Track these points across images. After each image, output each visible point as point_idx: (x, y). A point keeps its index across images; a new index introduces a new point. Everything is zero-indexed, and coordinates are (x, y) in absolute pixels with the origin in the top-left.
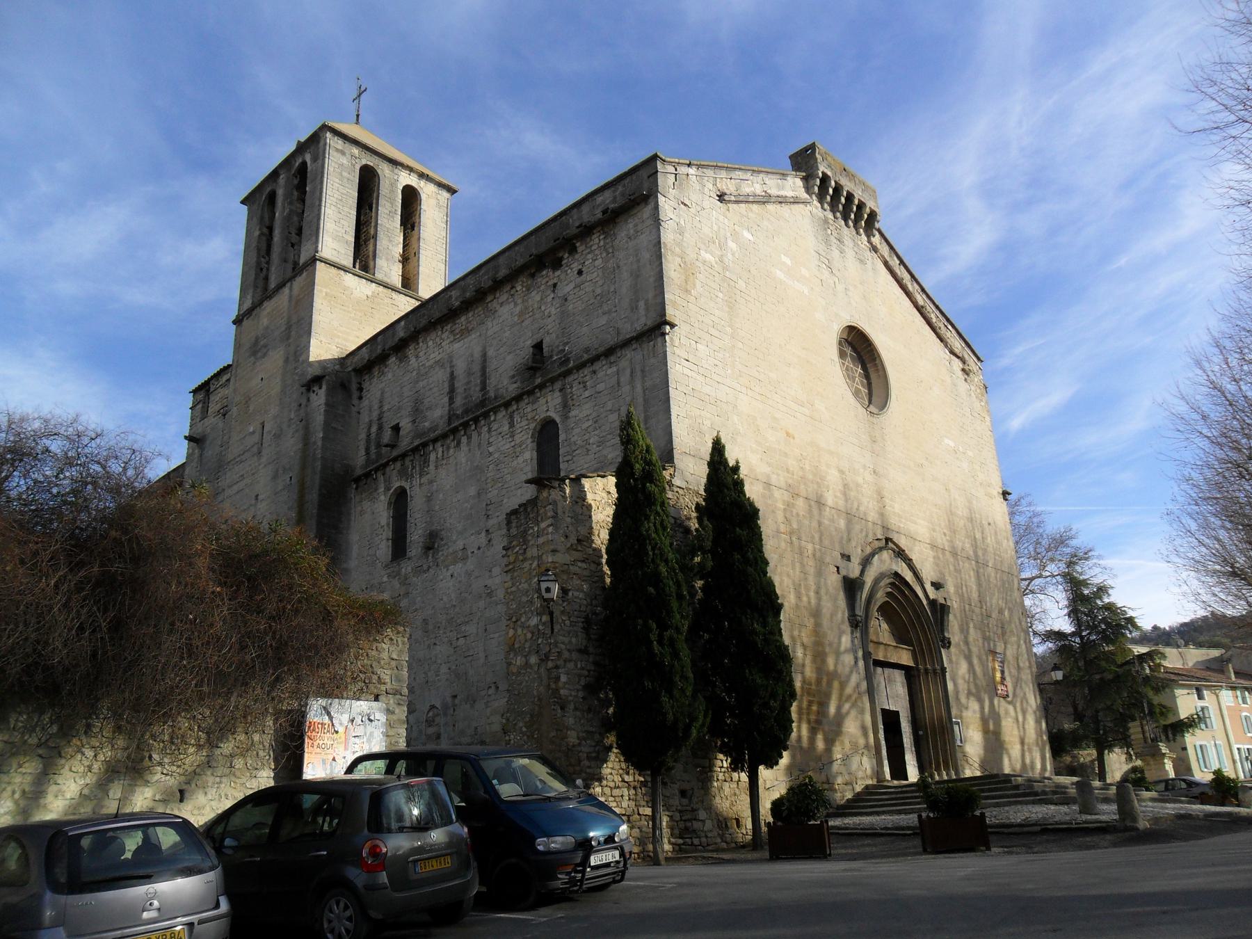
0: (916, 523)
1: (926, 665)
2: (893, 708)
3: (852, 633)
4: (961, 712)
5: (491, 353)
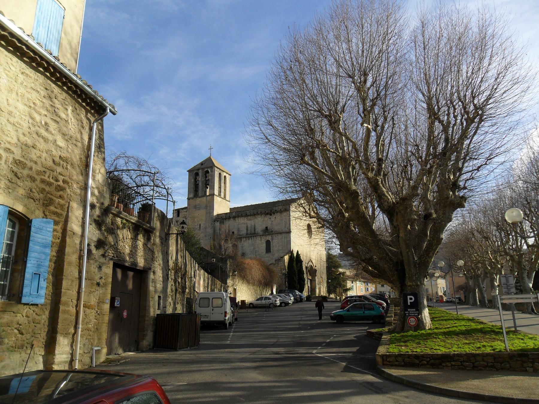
5: (256, 225)
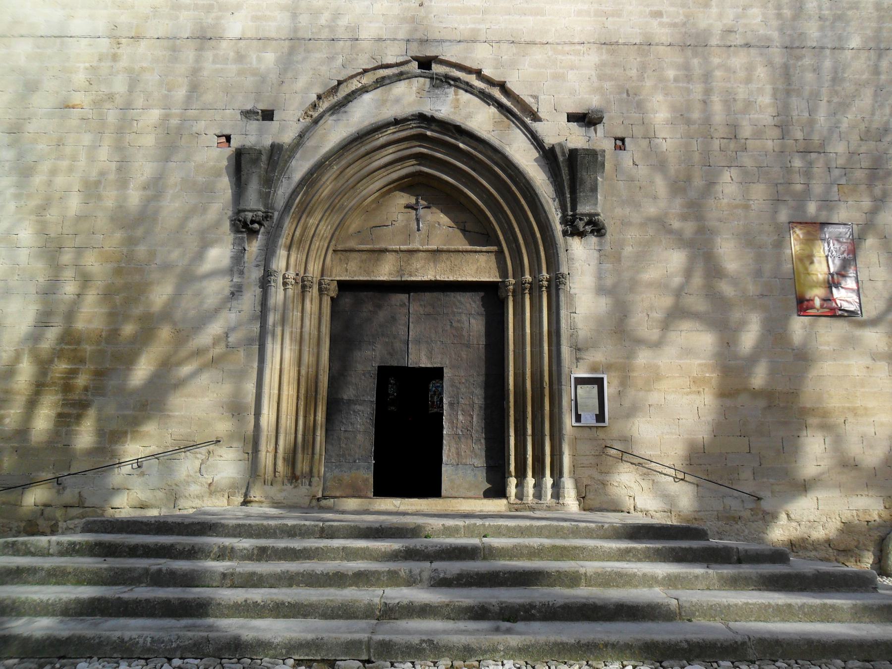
0: (538, 12)
1: (523, 274)
2: (420, 358)
3: (238, 242)
4: (630, 355)
